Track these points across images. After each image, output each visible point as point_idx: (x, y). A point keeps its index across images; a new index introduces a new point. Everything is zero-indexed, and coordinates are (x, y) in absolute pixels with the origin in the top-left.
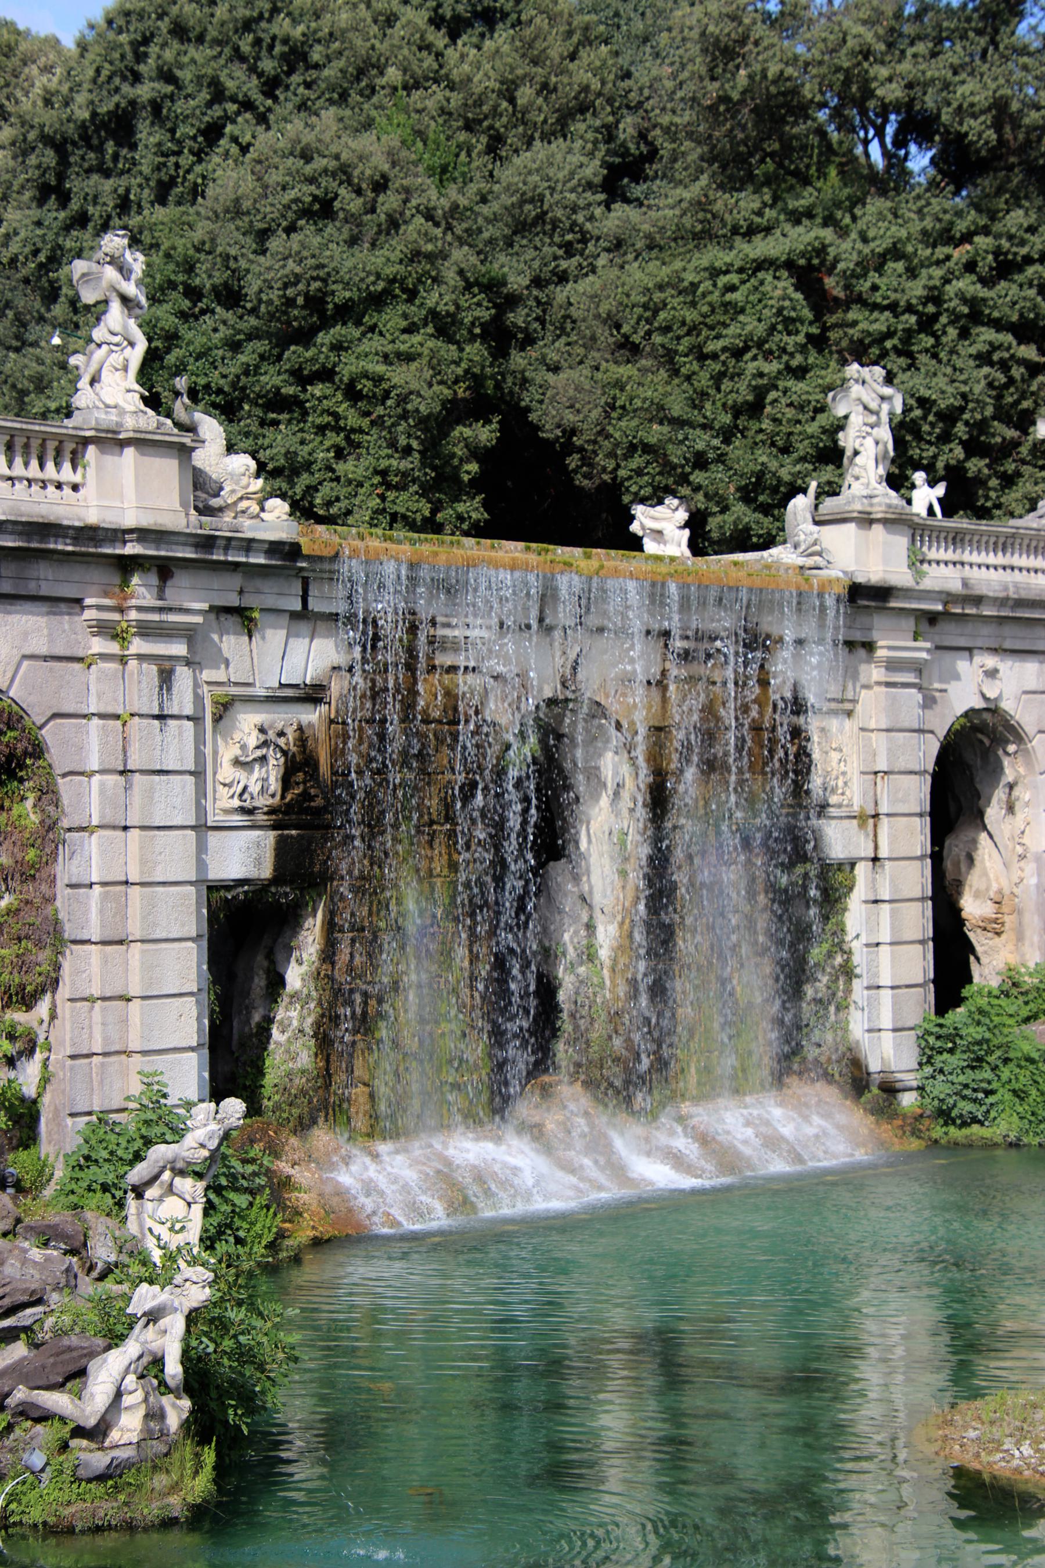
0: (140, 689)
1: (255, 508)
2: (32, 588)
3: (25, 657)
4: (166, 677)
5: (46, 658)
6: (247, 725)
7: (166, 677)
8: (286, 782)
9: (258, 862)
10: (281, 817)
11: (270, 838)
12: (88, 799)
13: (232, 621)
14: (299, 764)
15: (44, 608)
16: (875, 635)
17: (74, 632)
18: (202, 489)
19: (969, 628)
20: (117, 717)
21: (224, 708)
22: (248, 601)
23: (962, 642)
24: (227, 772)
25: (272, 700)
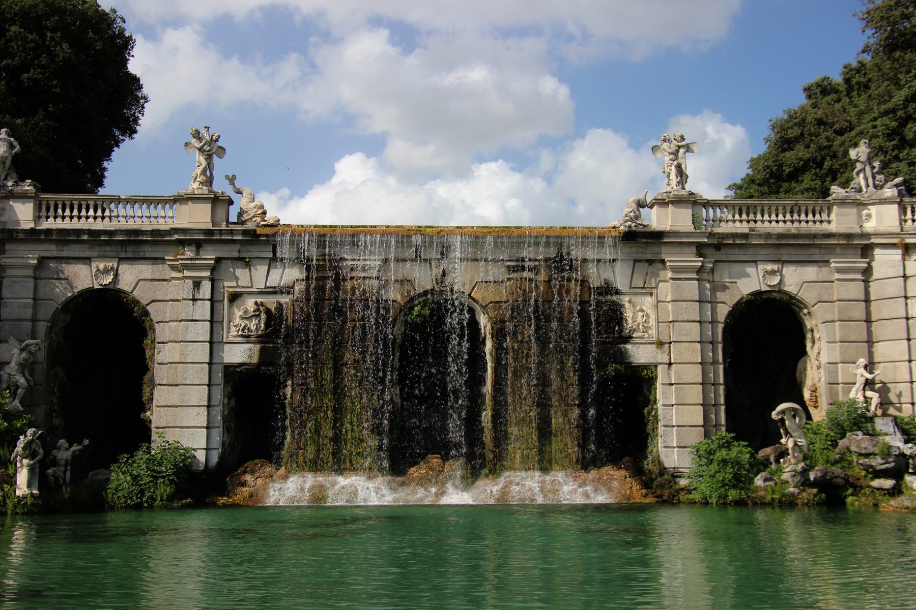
0: (185, 289)
1: (259, 219)
2: (142, 255)
3: (140, 280)
4: (197, 284)
5: (151, 280)
6: (250, 304)
7: (197, 284)
8: (267, 325)
9: (250, 357)
11: (258, 346)
12: (162, 332)
13: (239, 263)
14: (273, 318)
15: (150, 262)
16: (663, 256)
17: (163, 270)
19: (751, 251)
20: (177, 300)
21: (235, 297)
22: (243, 255)
23: (745, 258)
24: (237, 321)
25: (261, 293)
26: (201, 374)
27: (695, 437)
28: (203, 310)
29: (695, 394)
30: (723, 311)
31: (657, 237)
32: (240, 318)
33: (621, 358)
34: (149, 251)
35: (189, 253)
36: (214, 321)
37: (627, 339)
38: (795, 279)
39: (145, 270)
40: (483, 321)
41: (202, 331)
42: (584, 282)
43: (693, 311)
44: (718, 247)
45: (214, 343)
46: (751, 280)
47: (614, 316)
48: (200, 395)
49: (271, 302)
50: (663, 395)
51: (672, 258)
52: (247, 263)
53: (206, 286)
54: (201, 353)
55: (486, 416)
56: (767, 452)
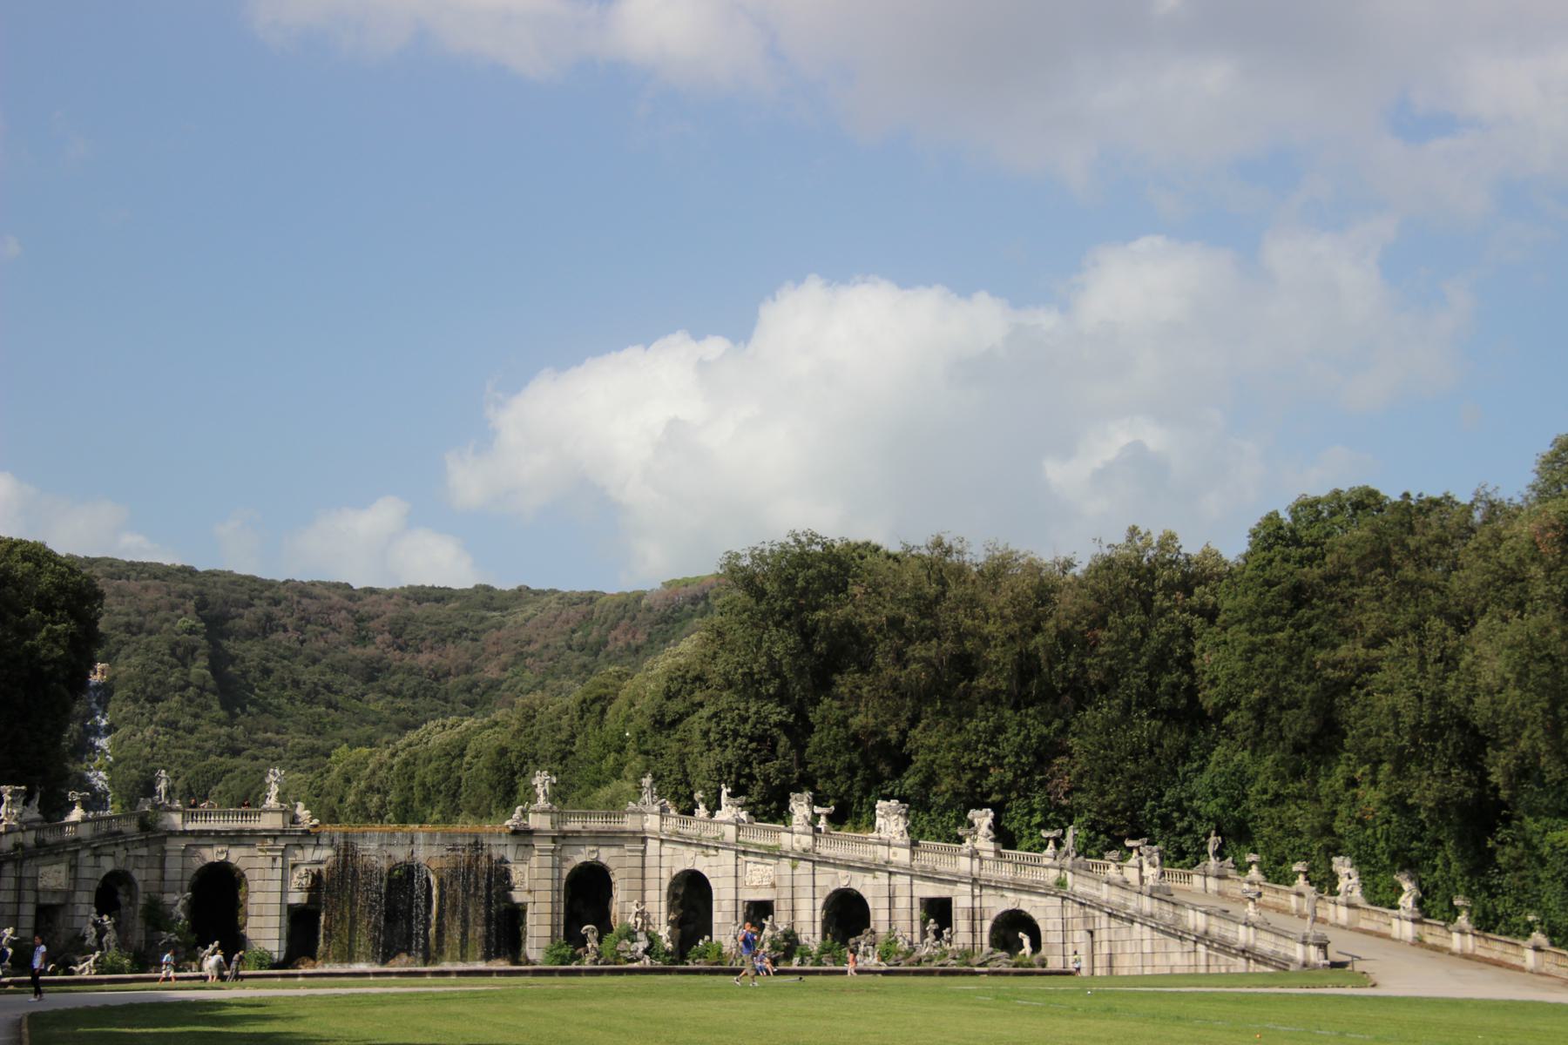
4: (274, 859)
6: (303, 870)
7: (274, 859)
10: (309, 890)
12: (253, 886)
14: (317, 878)
17: (254, 851)
18: (294, 820)
21: (294, 866)
26: (276, 910)
27: (546, 943)
28: (278, 874)
29: (547, 919)
30: (566, 872)
31: (530, 833)
32: (299, 879)
33: (508, 898)
34: (246, 841)
35: (270, 842)
36: (284, 880)
37: (512, 889)
38: (606, 855)
39: (243, 851)
40: (433, 878)
41: (277, 886)
42: (490, 857)
43: (548, 873)
44: (564, 837)
45: (284, 892)
46: (582, 856)
47: (506, 875)
48: (275, 921)
49: (315, 868)
50: (530, 919)
51: (538, 844)
52: (301, 847)
53: (279, 860)
54: (276, 898)
55: (432, 930)
56: (581, 950)
